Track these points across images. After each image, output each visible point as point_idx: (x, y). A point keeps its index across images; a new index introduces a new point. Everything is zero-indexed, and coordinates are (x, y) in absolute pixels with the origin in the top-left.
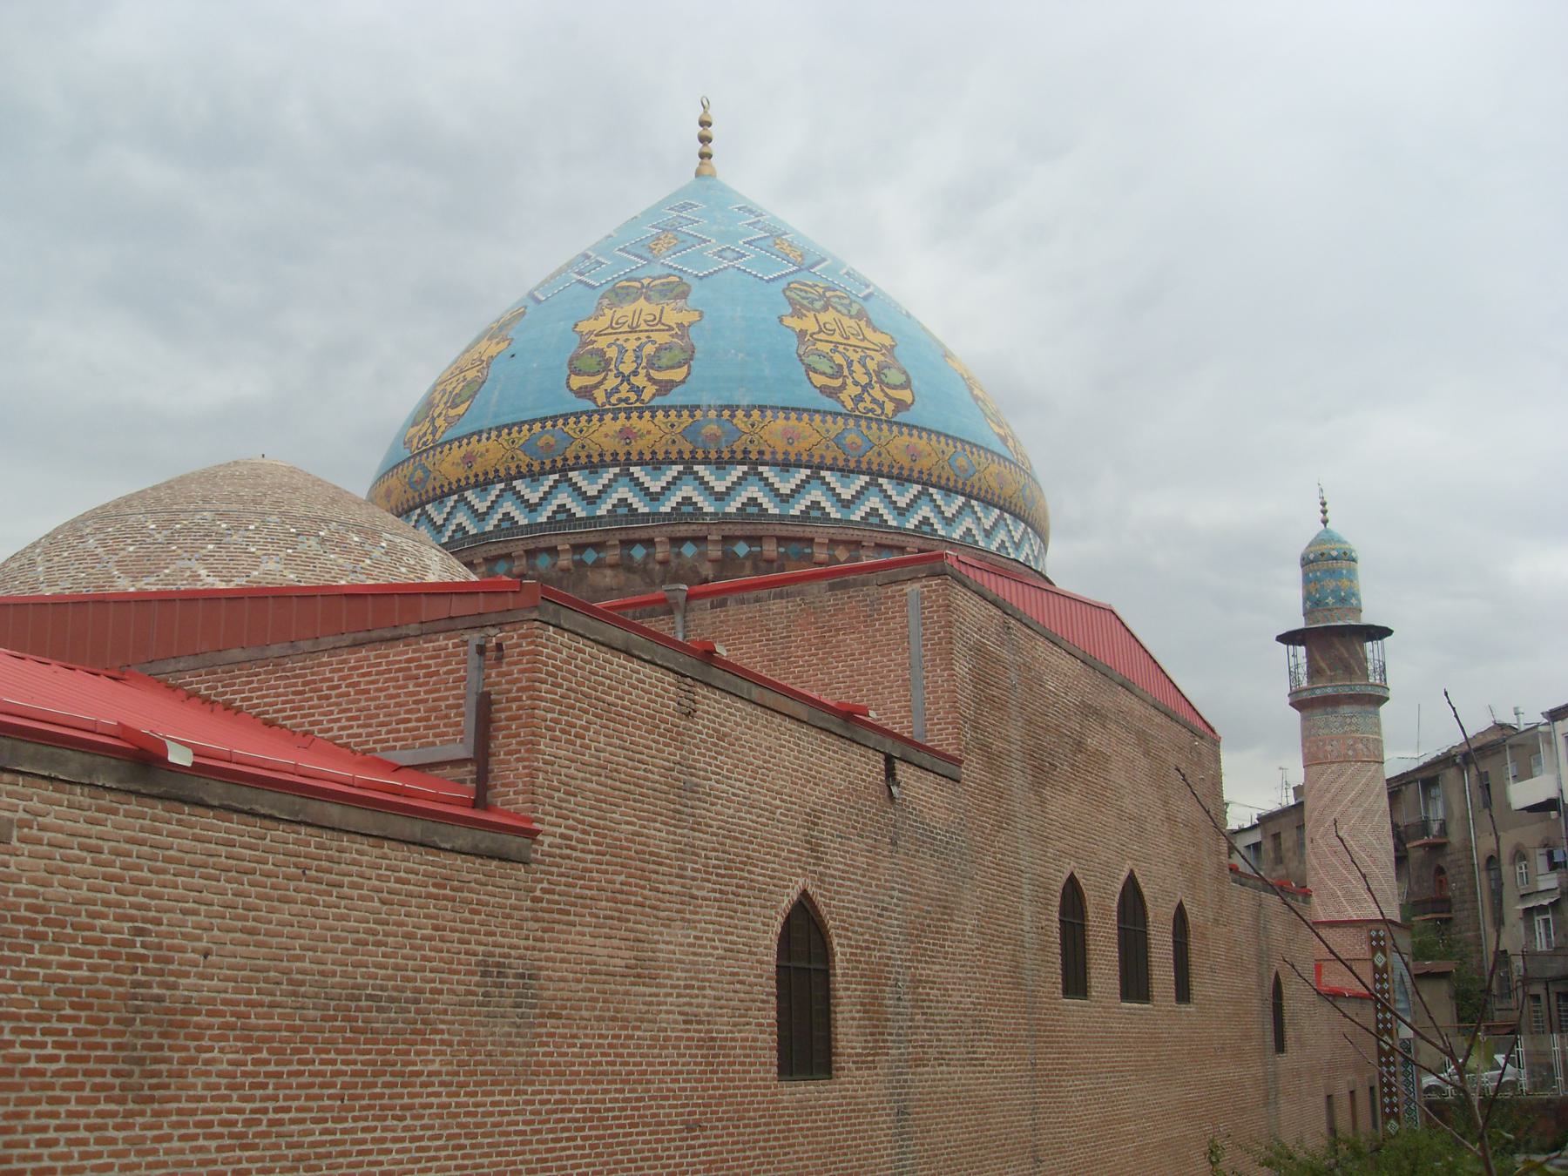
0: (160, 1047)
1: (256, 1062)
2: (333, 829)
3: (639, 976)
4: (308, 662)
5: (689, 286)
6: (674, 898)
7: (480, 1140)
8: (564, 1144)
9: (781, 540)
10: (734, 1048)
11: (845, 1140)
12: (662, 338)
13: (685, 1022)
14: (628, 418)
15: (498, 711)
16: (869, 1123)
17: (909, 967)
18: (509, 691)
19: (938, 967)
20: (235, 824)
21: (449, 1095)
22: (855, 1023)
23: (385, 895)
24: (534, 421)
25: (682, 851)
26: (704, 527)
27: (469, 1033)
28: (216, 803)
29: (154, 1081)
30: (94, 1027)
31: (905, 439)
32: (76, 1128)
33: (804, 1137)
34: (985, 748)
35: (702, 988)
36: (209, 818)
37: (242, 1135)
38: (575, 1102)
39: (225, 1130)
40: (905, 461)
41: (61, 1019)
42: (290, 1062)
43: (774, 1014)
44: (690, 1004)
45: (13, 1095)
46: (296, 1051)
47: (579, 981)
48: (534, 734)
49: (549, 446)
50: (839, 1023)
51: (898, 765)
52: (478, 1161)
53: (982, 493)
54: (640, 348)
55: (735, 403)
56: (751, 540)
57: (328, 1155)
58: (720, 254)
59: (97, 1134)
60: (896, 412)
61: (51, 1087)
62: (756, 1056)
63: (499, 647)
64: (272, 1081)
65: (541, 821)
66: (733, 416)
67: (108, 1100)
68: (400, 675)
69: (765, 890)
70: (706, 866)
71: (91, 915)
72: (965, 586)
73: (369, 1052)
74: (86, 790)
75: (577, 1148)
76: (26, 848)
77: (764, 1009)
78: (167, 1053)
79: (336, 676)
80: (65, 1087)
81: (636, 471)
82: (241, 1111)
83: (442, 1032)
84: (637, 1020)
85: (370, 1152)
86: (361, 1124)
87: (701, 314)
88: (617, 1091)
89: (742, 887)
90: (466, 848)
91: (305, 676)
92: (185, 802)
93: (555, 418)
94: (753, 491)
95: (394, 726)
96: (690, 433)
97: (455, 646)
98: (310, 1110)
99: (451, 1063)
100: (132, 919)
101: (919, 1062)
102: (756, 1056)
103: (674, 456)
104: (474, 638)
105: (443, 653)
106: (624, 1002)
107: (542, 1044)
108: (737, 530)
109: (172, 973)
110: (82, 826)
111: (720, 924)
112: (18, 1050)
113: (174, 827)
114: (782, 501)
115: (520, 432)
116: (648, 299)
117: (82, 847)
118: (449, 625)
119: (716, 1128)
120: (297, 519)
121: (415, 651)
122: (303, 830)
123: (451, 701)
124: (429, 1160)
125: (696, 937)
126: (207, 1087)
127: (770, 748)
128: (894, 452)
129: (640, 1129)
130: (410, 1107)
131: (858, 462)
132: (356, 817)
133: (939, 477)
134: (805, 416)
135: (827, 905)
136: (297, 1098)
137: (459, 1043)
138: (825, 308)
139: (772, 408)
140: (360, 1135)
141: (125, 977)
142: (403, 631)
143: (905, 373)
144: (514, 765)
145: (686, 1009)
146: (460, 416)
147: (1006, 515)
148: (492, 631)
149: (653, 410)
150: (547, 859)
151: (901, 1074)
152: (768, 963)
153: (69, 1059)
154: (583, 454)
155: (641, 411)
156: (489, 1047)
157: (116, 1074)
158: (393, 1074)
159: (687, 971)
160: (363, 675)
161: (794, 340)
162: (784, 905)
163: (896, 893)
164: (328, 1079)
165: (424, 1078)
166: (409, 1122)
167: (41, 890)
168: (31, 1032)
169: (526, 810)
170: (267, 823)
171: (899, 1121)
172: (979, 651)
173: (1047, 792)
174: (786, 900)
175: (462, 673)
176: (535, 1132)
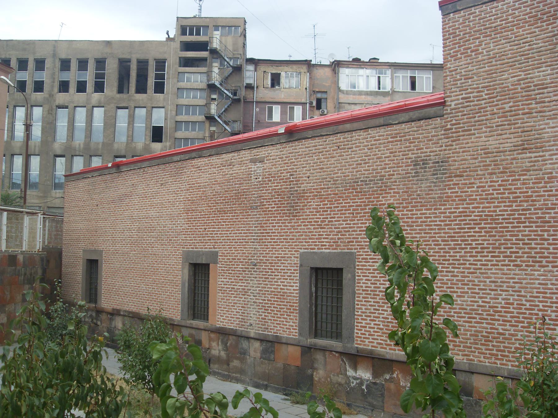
0: (298, 203)
1: (323, 205)
7: (415, 227)
20: (317, 140)
32: (279, 223)
36: (310, 141)
37: (321, 225)
39: (316, 224)
41: (275, 198)
42: (334, 204)
57: (349, 231)
61: (274, 214)
64: (329, 210)
67: (286, 216)
78: (299, 204)
80: (277, 214)
82: (320, 218)
86: (360, 222)
98: (342, 217)
99: (399, 200)
109: (300, 184)
112: (267, 206)
122: (339, 135)
126: (310, 212)
132: (356, 125)
136: (337, 214)
137: (402, 192)
140: (360, 225)
153: (277, 207)
156: (419, 192)
157: (288, 210)
164: (347, 208)
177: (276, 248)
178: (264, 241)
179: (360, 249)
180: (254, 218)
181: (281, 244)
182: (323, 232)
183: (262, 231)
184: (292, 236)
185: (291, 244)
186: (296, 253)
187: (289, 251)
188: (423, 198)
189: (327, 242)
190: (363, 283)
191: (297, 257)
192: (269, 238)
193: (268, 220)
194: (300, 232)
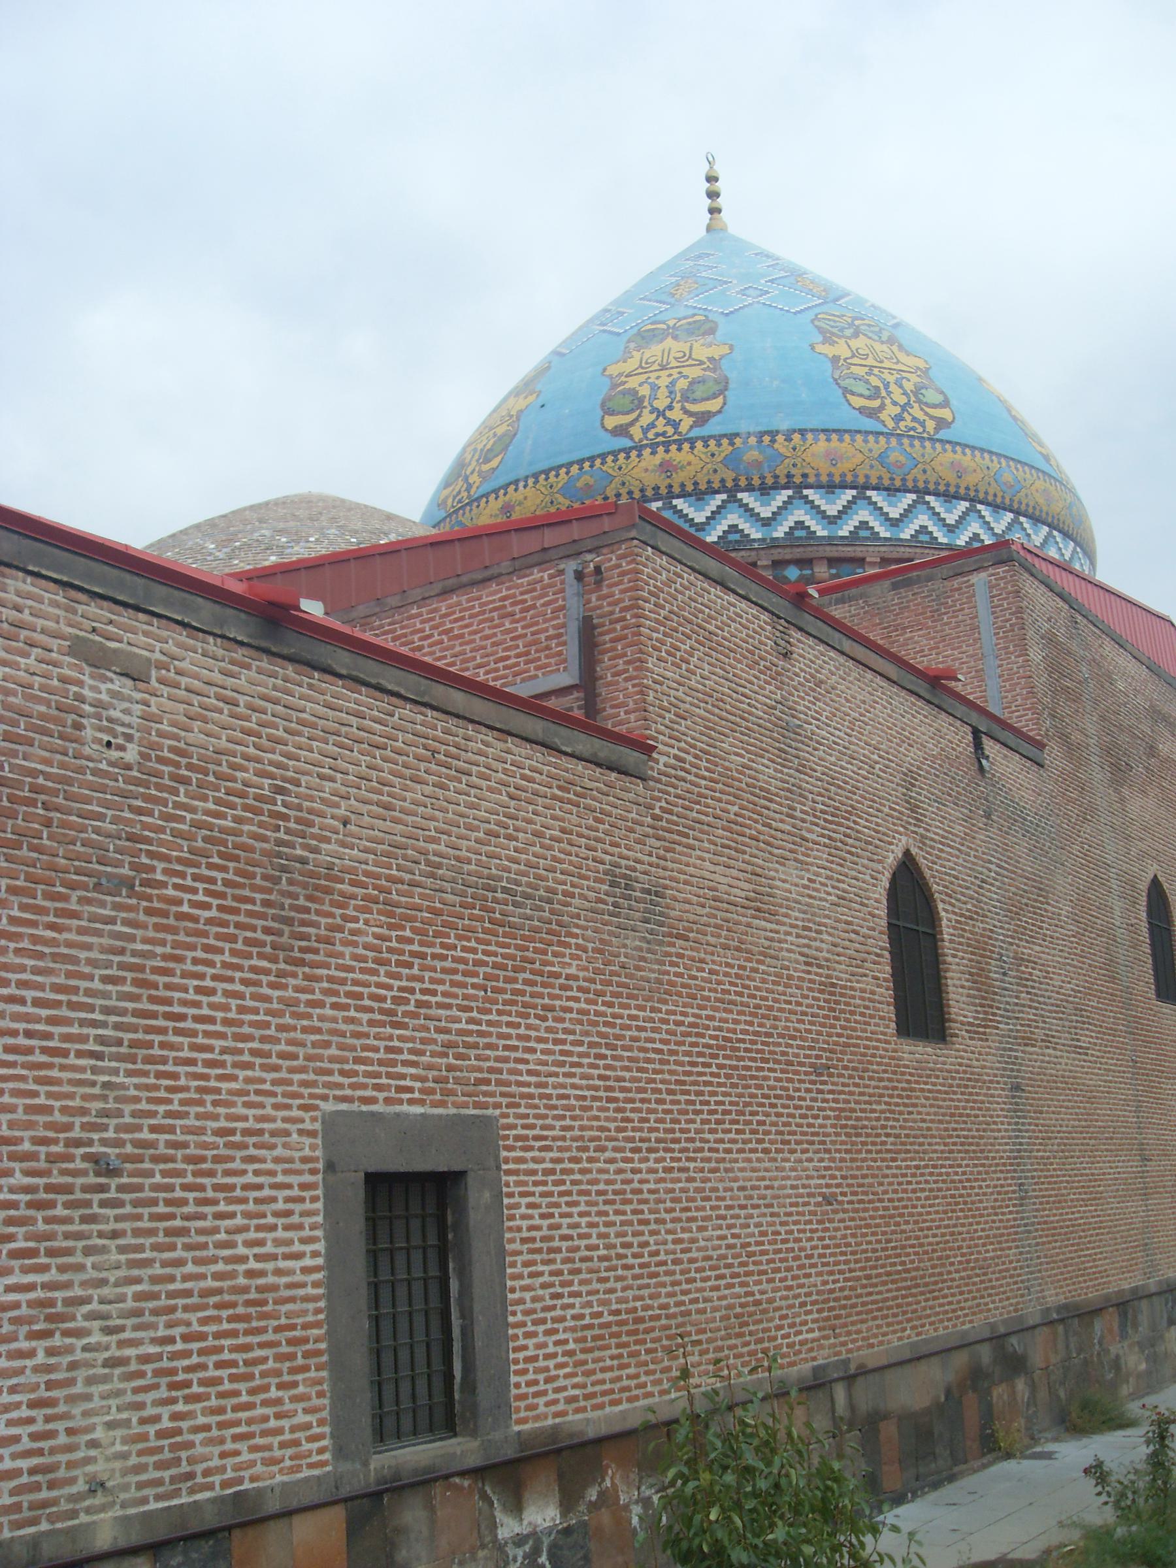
2: (458, 716)
3: (758, 910)
4: (397, 617)
5: (716, 323)
6: (786, 837)
8: (700, 1069)
9: (832, 562)
10: (854, 997)
11: (965, 1108)
12: (695, 372)
13: (807, 964)
14: (667, 451)
15: (602, 634)
16: (986, 1095)
17: (1011, 944)
18: (612, 613)
19: (1038, 948)
20: (363, 696)
21: (588, 1002)
22: (965, 991)
23: (512, 789)
24: (571, 464)
25: (789, 790)
26: (753, 553)
27: (602, 941)
28: (344, 672)
29: (304, 943)
30: (242, 880)
31: (949, 455)
33: (927, 1098)
34: (1064, 737)
35: (817, 932)
36: (338, 687)
38: (707, 1028)
39: (375, 1005)
40: (951, 477)
41: (210, 866)
42: (432, 945)
43: (888, 969)
44: (809, 946)
45: (169, 937)
46: (437, 934)
47: (703, 906)
48: (641, 652)
49: (588, 486)
50: (951, 989)
51: (985, 739)
52: (619, 1073)
53: (1030, 510)
54: (673, 383)
55: (774, 428)
56: (802, 563)
57: (475, 1046)
58: (743, 292)
59: (252, 989)
60: (937, 429)
61: (205, 934)
62: (875, 1009)
63: (598, 570)
64: (417, 961)
65: (655, 739)
66: (773, 441)
67: (261, 956)
68: (495, 614)
69: (870, 843)
70: (814, 809)
71: (233, 766)
72: (1032, 575)
73: (508, 946)
74: (219, 640)
75: (712, 1074)
76: (165, 690)
77: (879, 963)
79: (427, 626)
80: (218, 937)
81: (679, 503)
83: (576, 936)
84: (761, 953)
85: (515, 1048)
86: (505, 1018)
87: (731, 347)
88: (746, 1022)
89: (849, 836)
90: (586, 755)
91: (395, 630)
92: (315, 668)
93: (592, 459)
94: (799, 514)
95: (493, 665)
96: (731, 461)
97: (551, 577)
98: (455, 996)
99: (587, 969)
100: (272, 776)
101: (1028, 1041)
102: (875, 1009)
103: (716, 485)
104: (571, 566)
105: (538, 586)
106: (746, 934)
107: (672, 964)
108: (787, 554)
110: (217, 677)
111: (831, 870)
112: (170, 892)
113: (304, 690)
114: (830, 523)
115: (557, 476)
116: (675, 338)
117: (219, 698)
118: (543, 557)
119: (843, 1076)
120: (356, 532)
121: (508, 589)
122: (429, 712)
123: (551, 632)
124: (573, 1065)
125: (810, 880)
126: (355, 957)
127: (864, 702)
128: (939, 468)
129: (771, 1065)
130: (551, 1009)
131: (904, 480)
133: (986, 493)
134: (847, 437)
135: (931, 869)
138: (856, 334)
139: (812, 430)
140: (505, 1030)
141: (269, 833)
142: (495, 571)
143: (942, 393)
144: (623, 684)
145: (805, 950)
146: (494, 470)
147: (1055, 533)
148: (589, 557)
149: (692, 442)
150: (664, 779)
151: (1011, 1050)
152: (879, 917)
154: (624, 491)
155: (679, 444)
156: (622, 959)
157: (267, 931)
158: (533, 972)
159: (805, 912)
160: (456, 620)
161: (829, 366)
162: (890, 861)
163: (993, 867)
164: (470, 967)
165: (562, 981)
166: (550, 1023)
167: (183, 734)
168: (183, 875)
169: (639, 728)
170: (394, 700)
171: (1014, 1097)
172: (1050, 639)
173: (1125, 791)
174: (891, 856)
175: (561, 602)
176: (672, 1052)
177: (218, 1091)
178: (156, 1051)
179: (508, 1106)
180: (98, 933)
181: (242, 1074)
182: (401, 1038)
183: (145, 1005)
184: (290, 1042)
185: (283, 1074)
186: (307, 1116)
187: (276, 1107)
188: (630, 976)
189: (415, 1078)
190: (523, 1217)
191: (312, 1134)
192: (186, 1041)
193: (179, 959)
194: (319, 1031)
